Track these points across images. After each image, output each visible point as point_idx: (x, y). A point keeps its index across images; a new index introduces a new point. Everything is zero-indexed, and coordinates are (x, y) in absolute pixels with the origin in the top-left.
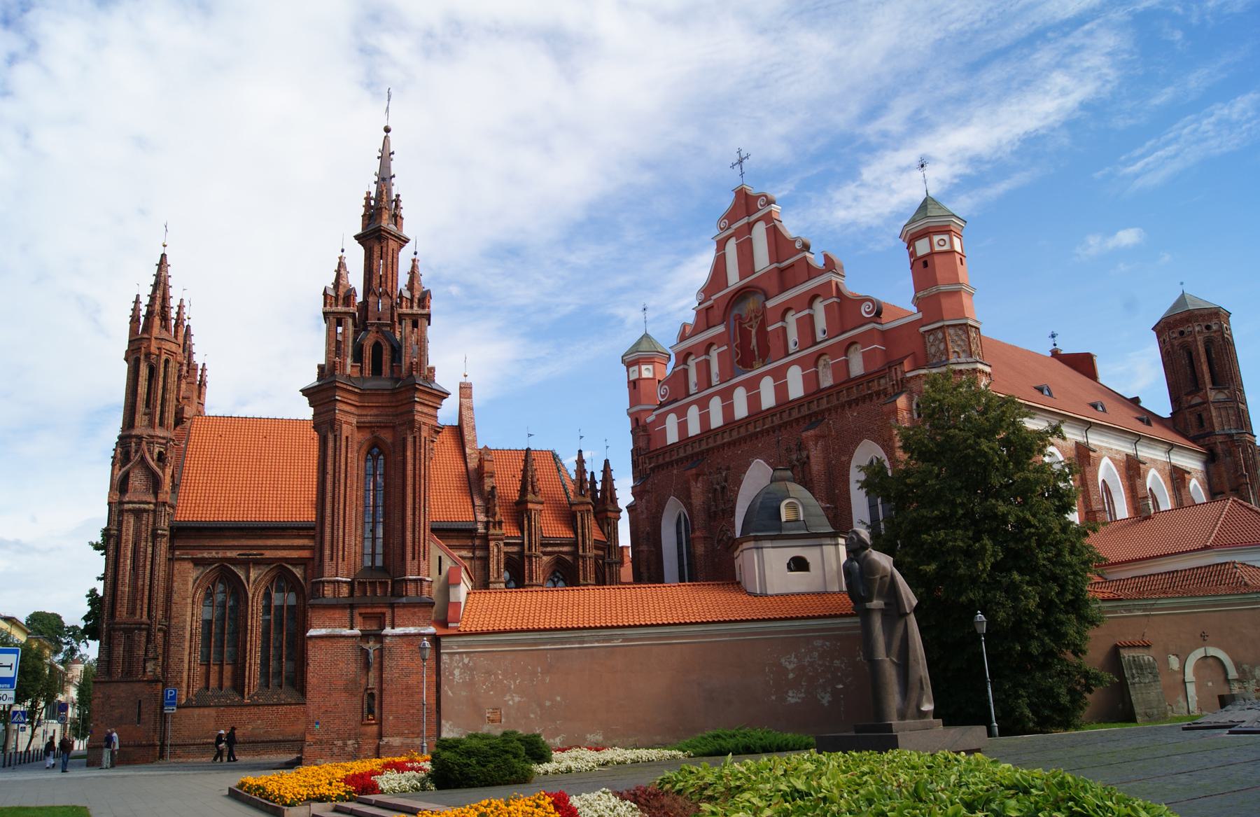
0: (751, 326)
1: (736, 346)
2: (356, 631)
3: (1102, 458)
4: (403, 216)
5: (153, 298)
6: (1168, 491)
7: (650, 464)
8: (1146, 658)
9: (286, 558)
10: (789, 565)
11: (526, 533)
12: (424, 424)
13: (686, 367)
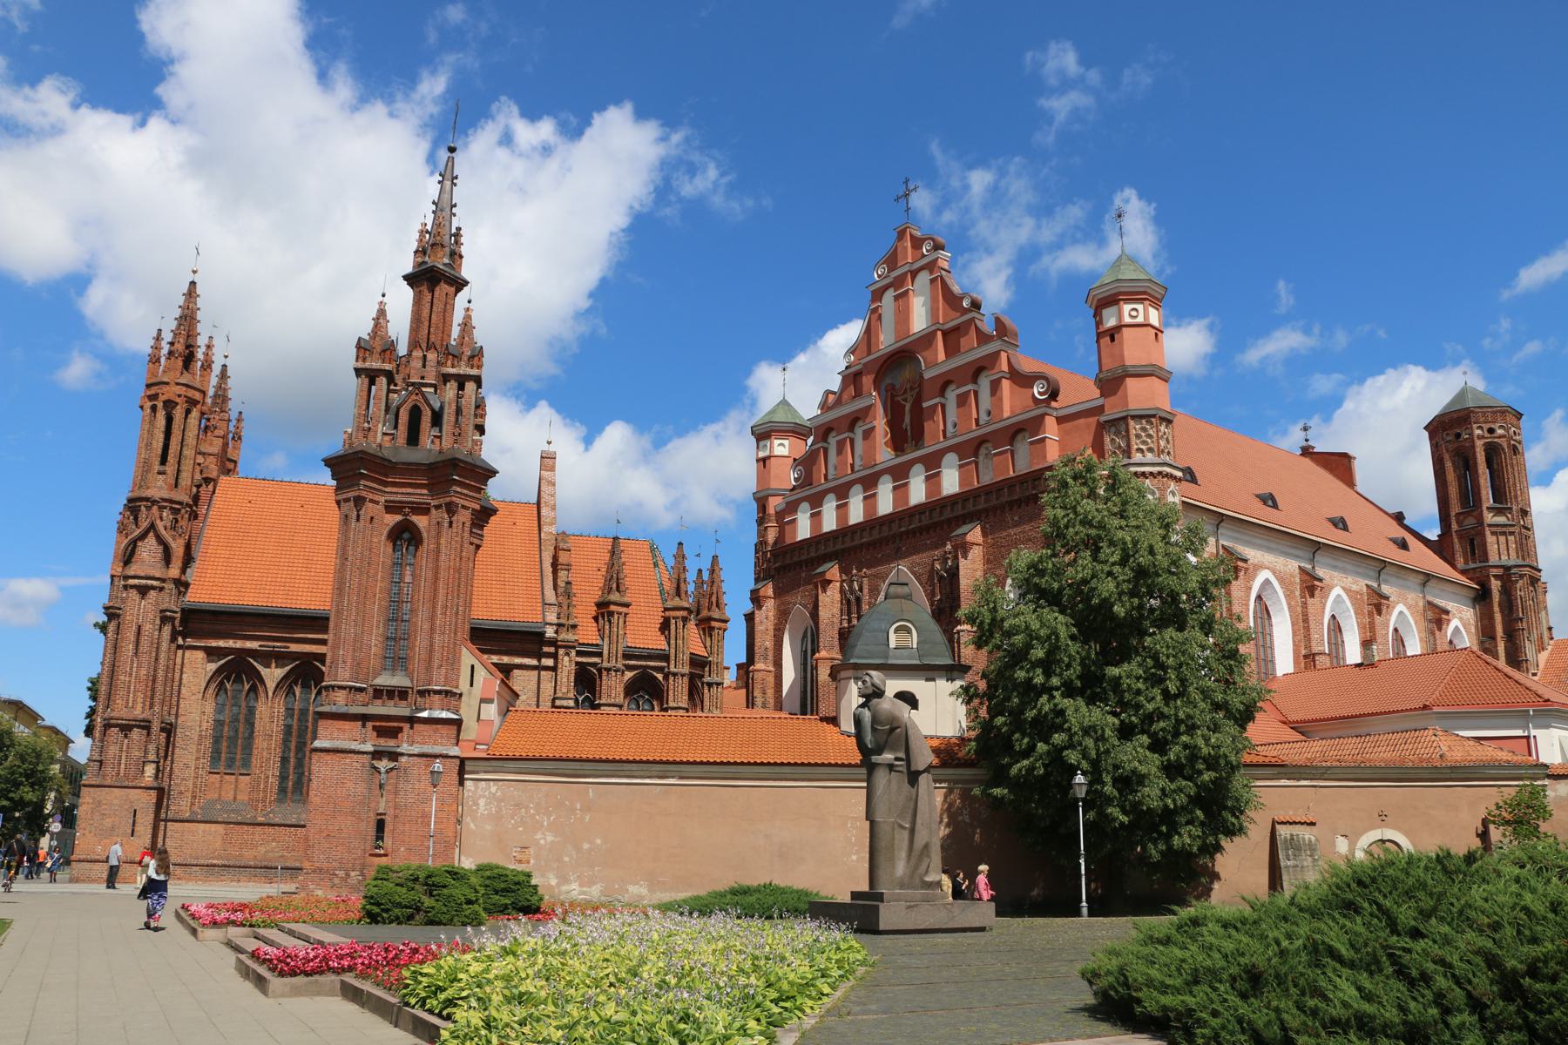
2: (369, 747)
3: (1333, 588)
4: (463, 254)
5: (176, 334)
6: (1419, 632)
7: (775, 563)
8: (1307, 837)
11: (606, 640)
12: (463, 507)
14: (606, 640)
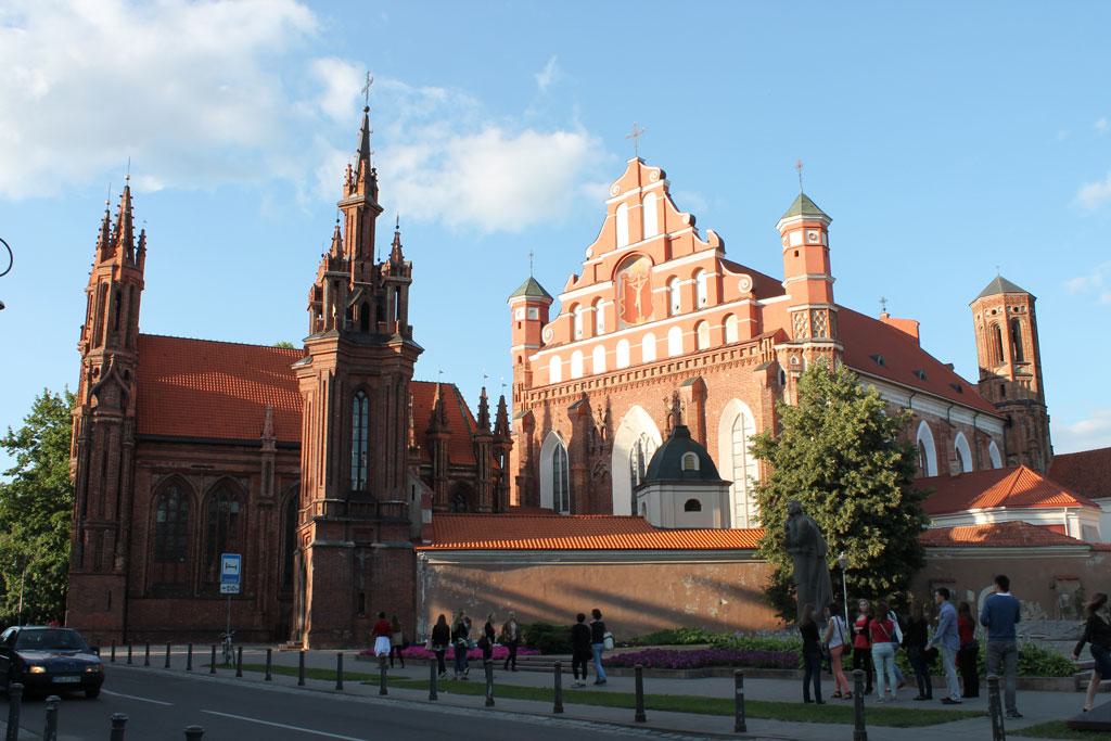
0: (637, 286)
9: (233, 472)
10: (686, 506)
14: (435, 460)
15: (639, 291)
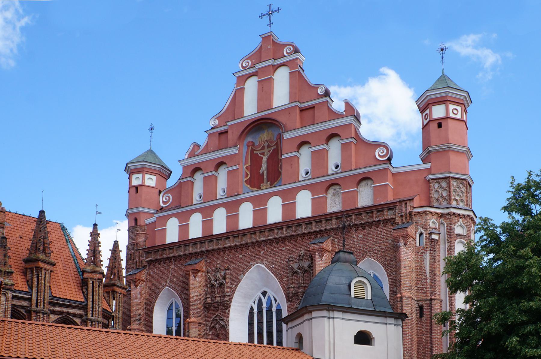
1: (246, 168)
13: (192, 180)
15: (265, 159)
